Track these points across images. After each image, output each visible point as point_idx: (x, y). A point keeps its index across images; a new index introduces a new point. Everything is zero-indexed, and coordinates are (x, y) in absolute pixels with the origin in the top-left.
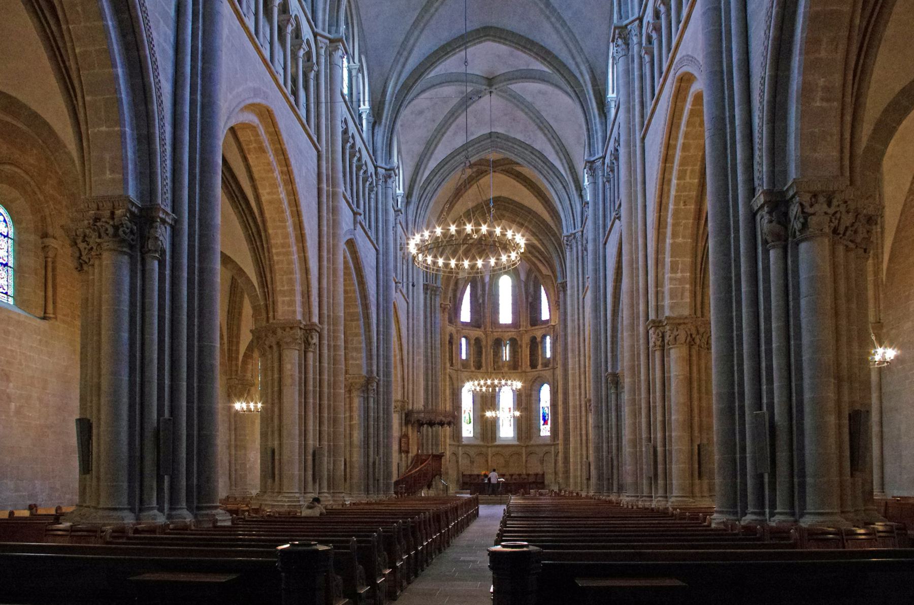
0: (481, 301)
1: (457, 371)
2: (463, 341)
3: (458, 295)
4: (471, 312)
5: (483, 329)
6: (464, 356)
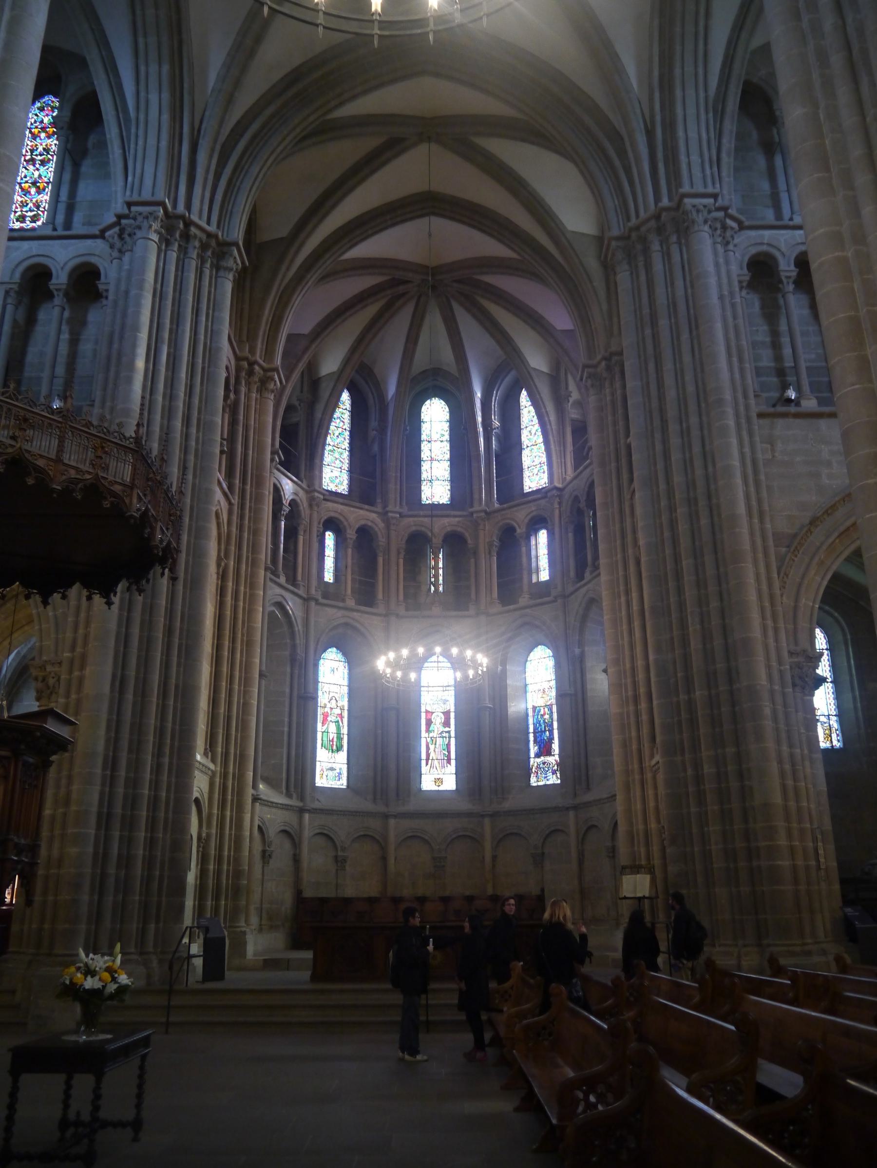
0: (376, 448)
1: (306, 600)
2: (330, 539)
3: (318, 415)
4: (351, 471)
5: (379, 509)
6: (329, 577)
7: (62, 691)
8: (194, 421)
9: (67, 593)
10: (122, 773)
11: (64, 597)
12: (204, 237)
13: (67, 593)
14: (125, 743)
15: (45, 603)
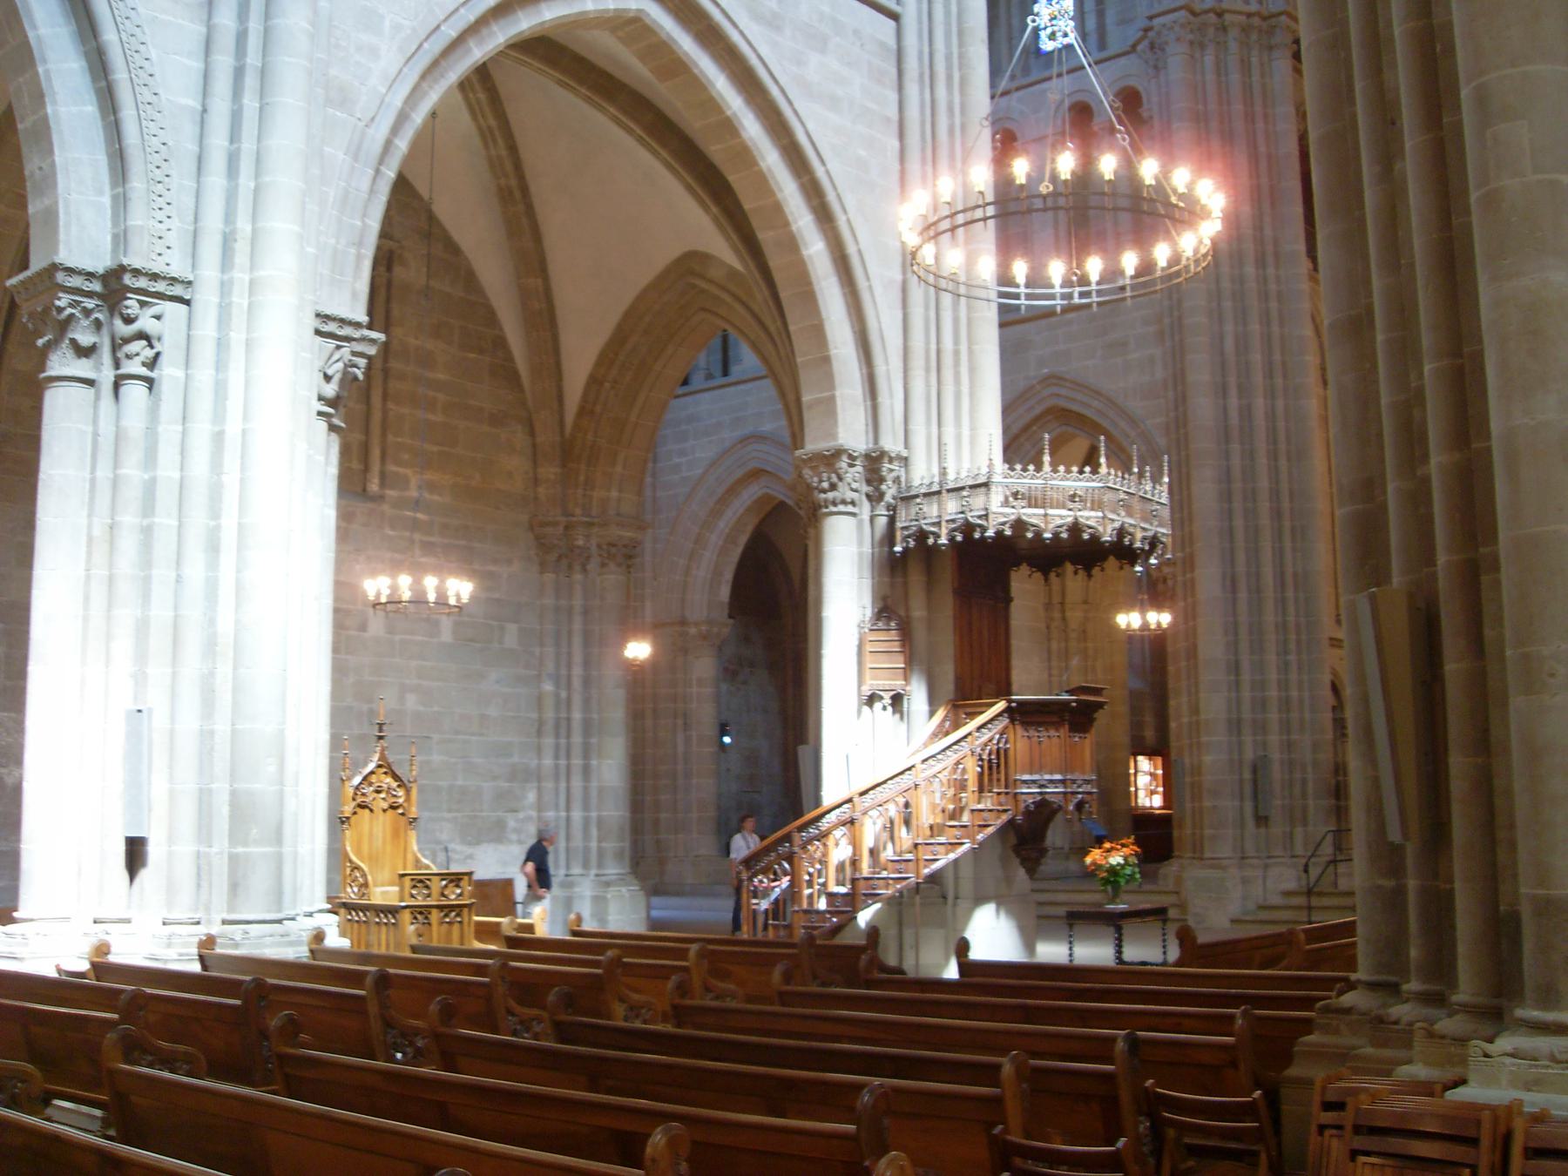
7: (1179, 590)
8: (1270, 259)
9: (1104, 566)
10: (1246, 677)
11: (1103, 570)
12: (1243, 18)
13: (1104, 566)
14: (1244, 646)
15: (1090, 576)
